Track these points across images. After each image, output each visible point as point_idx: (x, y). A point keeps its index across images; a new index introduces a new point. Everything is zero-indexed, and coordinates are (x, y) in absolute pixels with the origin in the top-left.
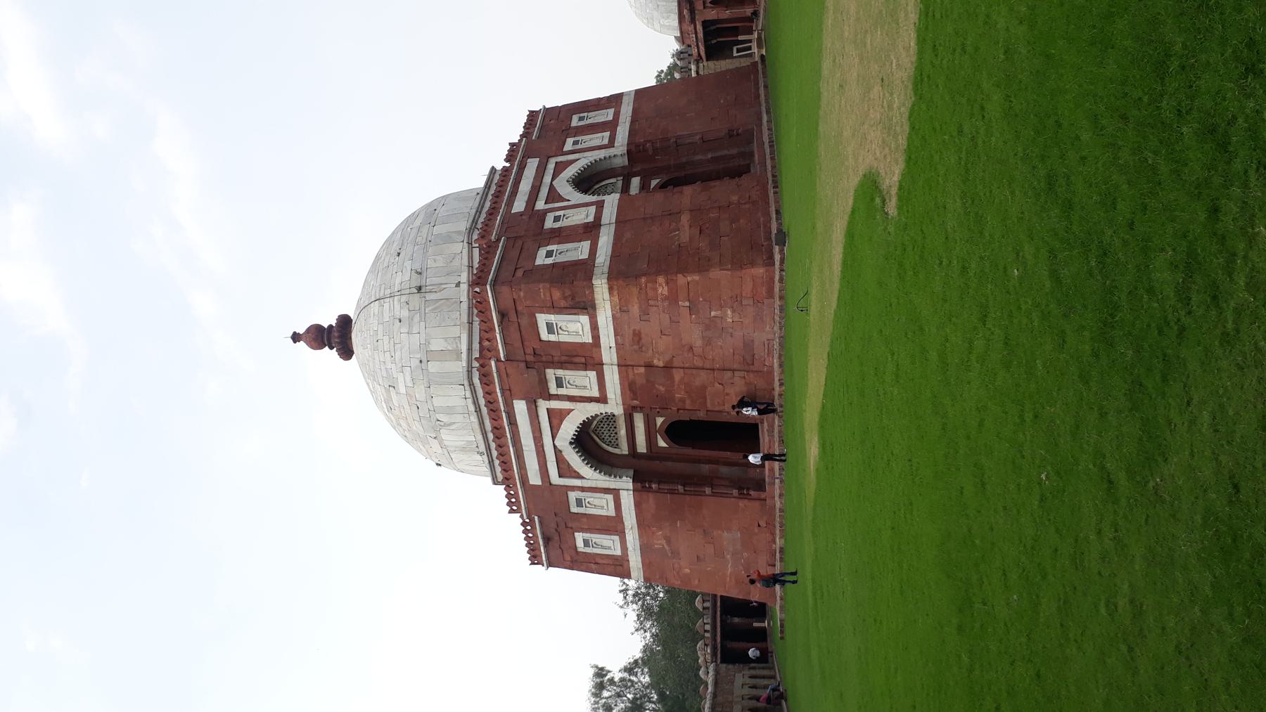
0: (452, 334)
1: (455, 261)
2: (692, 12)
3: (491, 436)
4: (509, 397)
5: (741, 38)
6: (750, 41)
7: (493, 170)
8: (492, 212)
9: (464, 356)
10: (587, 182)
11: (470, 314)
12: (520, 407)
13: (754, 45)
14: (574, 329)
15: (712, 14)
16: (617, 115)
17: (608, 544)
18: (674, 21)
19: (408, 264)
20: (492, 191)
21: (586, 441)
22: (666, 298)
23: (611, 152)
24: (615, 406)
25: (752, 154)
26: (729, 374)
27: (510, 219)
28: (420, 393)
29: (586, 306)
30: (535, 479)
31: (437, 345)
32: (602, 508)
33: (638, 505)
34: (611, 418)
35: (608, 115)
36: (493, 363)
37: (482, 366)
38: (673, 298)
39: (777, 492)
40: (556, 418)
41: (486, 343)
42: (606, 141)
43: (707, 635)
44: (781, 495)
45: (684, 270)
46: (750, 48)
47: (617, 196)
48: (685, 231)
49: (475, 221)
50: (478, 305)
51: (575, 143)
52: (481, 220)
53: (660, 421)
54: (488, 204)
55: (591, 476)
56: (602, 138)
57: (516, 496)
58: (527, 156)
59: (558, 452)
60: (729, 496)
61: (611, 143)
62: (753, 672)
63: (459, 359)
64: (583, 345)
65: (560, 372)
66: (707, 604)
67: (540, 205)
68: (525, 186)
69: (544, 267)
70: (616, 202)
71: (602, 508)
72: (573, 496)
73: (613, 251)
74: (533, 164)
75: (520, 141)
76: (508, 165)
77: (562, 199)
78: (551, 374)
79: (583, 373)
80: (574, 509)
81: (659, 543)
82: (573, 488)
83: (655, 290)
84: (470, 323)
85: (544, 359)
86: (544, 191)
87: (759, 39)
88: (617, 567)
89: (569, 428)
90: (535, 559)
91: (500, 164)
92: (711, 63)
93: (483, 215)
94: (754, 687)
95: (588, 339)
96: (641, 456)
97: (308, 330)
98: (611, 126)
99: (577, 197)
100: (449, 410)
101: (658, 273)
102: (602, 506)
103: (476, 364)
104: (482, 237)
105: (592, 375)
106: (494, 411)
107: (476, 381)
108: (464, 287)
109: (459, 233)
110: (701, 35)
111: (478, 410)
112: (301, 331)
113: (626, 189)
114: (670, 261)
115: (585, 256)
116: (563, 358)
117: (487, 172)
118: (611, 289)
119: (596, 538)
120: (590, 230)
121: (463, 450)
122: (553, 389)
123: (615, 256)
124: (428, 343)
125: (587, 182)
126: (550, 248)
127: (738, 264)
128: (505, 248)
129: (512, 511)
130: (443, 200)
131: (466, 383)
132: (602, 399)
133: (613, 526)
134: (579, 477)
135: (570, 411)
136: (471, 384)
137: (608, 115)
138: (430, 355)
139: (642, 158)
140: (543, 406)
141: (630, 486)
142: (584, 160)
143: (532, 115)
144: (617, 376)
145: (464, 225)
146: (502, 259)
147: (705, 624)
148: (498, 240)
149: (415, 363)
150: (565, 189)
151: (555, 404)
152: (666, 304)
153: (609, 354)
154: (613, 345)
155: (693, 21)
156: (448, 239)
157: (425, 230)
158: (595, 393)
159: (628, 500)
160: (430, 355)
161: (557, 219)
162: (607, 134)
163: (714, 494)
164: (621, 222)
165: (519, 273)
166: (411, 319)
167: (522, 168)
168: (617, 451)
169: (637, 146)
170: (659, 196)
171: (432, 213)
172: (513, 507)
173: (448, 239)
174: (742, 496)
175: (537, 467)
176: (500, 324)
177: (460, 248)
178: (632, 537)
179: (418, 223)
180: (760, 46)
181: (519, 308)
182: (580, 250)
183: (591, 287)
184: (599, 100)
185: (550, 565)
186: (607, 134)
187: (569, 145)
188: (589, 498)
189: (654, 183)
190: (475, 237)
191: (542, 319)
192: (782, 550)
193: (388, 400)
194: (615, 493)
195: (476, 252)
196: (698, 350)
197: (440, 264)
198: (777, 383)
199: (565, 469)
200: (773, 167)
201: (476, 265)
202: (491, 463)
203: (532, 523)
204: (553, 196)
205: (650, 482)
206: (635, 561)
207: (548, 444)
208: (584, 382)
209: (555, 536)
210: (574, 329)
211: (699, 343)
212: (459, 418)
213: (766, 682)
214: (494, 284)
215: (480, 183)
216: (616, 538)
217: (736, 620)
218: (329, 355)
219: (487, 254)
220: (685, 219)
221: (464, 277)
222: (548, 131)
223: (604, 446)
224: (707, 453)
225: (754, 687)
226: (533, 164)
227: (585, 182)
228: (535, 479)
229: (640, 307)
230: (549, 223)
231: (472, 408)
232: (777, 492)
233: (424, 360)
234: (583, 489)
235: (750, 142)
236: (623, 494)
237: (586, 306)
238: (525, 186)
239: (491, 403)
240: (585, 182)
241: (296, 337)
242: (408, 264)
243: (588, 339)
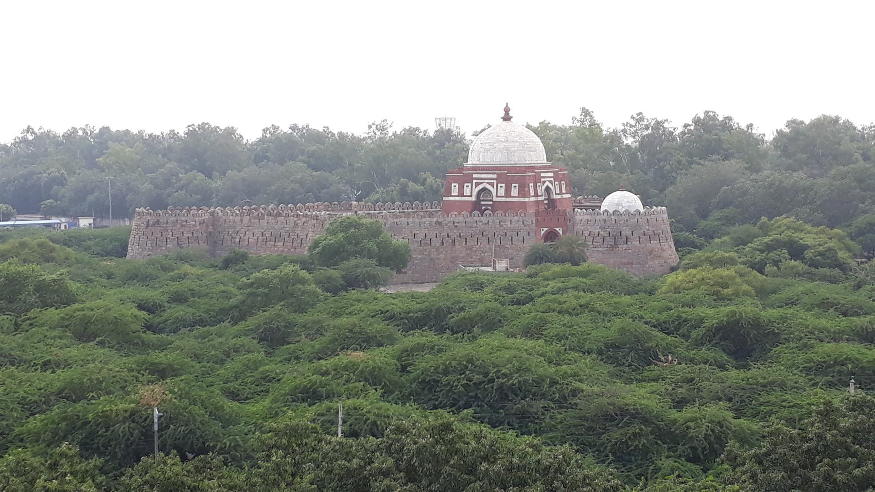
4: (498, 174)
10: (548, 189)
12: (495, 176)
14: (515, 192)
55: (476, 191)
56: (558, 192)
72: (469, 185)
89: (489, 187)
98: (561, 193)
99: (544, 188)
102: (467, 191)
120: (536, 195)
122: (499, 185)
125: (548, 189)
133: (461, 194)
140: (495, 182)
150: (545, 185)
178: (457, 199)
194: (471, 196)
199: (477, 184)
204: (544, 182)
208: (502, 192)
228: (475, 176)
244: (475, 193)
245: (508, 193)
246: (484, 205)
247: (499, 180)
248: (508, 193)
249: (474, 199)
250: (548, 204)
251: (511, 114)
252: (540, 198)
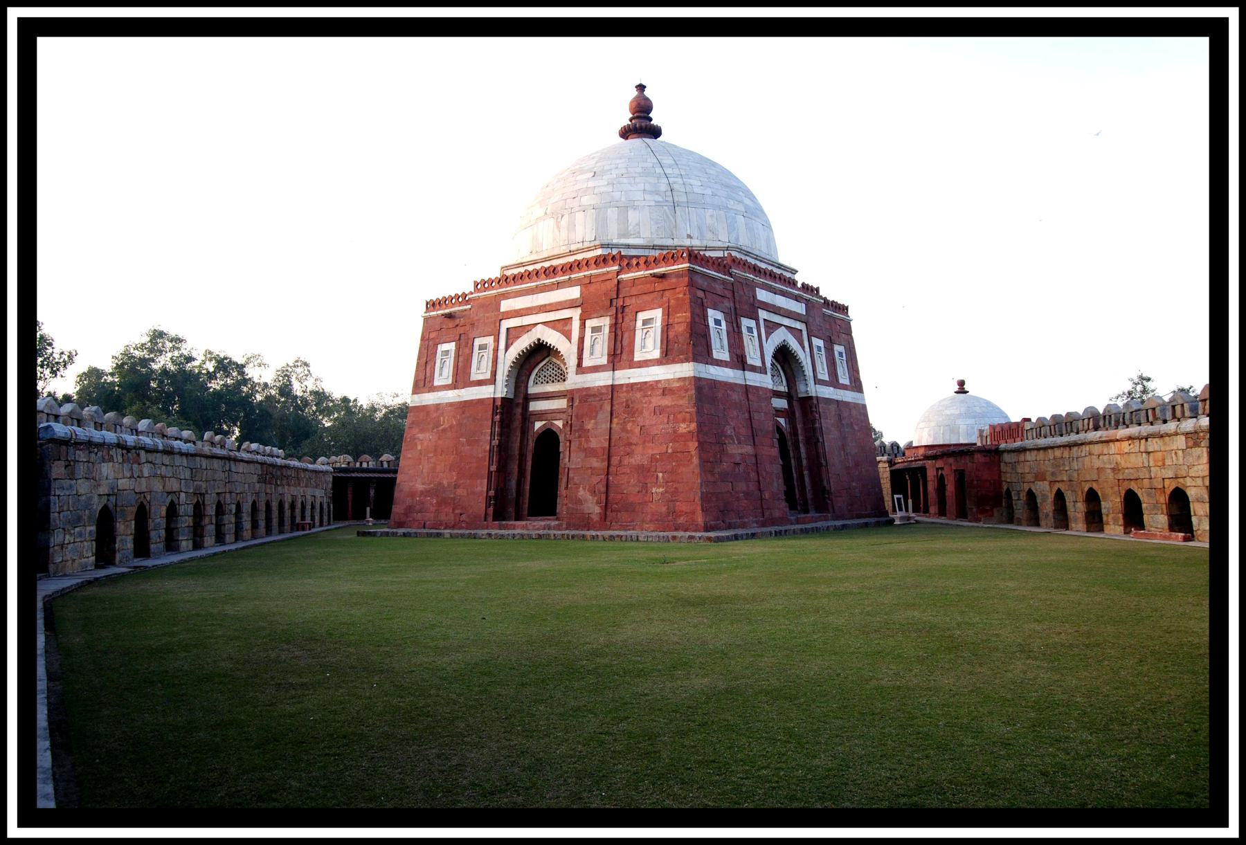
0: (642, 230)
1: (711, 233)
2: (935, 457)
3: (547, 265)
4: (586, 283)
5: (910, 501)
6: (907, 510)
7: (794, 272)
8: (756, 270)
9: (623, 241)
11: (661, 247)
12: (574, 293)
13: (903, 514)
14: (648, 343)
15: (931, 474)
16: (844, 387)
17: (443, 375)
18: (926, 440)
19: (708, 192)
20: (775, 270)
21: (540, 351)
22: (675, 432)
23: (811, 382)
24: (574, 381)
25: (807, 511)
26: (604, 489)
27: (752, 286)
28: (586, 200)
29: (668, 355)
30: (506, 305)
31: (633, 216)
32: (478, 369)
33: (481, 402)
34: (562, 377)
35: (844, 379)
36: (616, 268)
37: (613, 258)
38: (676, 437)
39: (493, 532)
40: (562, 326)
41: (634, 262)
42: (820, 377)
43: (358, 465)
44: (490, 535)
45: (702, 447)
46: (901, 510)
47: (770, 387)
48: (739, 450)
49: (748, 253)
50: (671, 255)
51: (819, 348)
52: (749, 260)
53: (559, 424)
54: (763, 266)
56: (824, 375)
57: (491, 287)
58: (807, 302)
60: (488, 489)
61: (817, 381)
62: (325, 506)
63: (620, 236)
64: (632, 352)
65: (607, 330)
66: (385, 465)
67: (763, 314)
68: (780, 301)
69: (705, 317)
70: (764, 385)
71: (478, 369)
73: (720, 382)
74: (800, 308)
75: (821, 297)
76: (799, 285)
77: (768, 335)
78: (605, 322)
79: (606, 352)
81: (446, 422)
82: (497, 341)
83: (684, 421)
84: (654, 247)
85: (620, 315)
86: (776, 319)
87: (909, 518)
88: (423, 382)
89: (553, 338)
90: (431, 305)
91: (800, 279)
92: (888, 475)
93: (753, 262)
94: (313, 507)
95: (638, 357)
96: (526, 407)
97: (647, 99)
98: (834, 382)
99: (769, 350)
100: (572, 226)
101: (700, 426)
102: (480, 370)
103: (615, 252)
104: (734, 260)
105: (604, 361)
106: (570, 268)
107: (599, 252)
108: (687, 243)
109: (737, 239)
110: (914, 465)
111: (571, 253)
112: (647, 93)
113: (778, 394)
114: (710, 437)
115: (716, 355)
116: (619, 333)
117: (793, 266)
118: (684, 379)
119: (450, 362)
120: (739, 361)
121: (535, 239)
122: (589, 323)
123: (714, 384)
124: (635, 208)
126: (723, 323)
127: (705, 498)
128: (724, 282)
129: (476, 284)
130: (767, 226)
131: (597, 243)
132: (580, 368)
134: (507, 348)
135: (569, 338)
136: (596, 248)
137: (844, 379)
138: (624, 209)
139: (804, 409)
141: (499, 395)
142: (803, 356)
143: (843, 309)
144: (602, 383)
145: (744, 242)
146: (714, 279)
147: (368, 462)
148: (731, 275)
149: (617, 195)
150: (779, 336)
151: (576, 325)
152: (670, 431)
153: (625, 376)
154: (632, 381)
155: (926, 458)
156: (732, 227)
157: (741, 208)
159: (486, 392)
160: (624, 209)
161: (750, 330)
162: (826, 378)
163: (490, 473)
164: (747, 389)
165: (700, 294)
166: (657, 193)
167: (797, 298)
168: (531, 382)
169: (817, 406)
170: (769, 426)
171: (755, 213)
172: (481, 285)
173: (732, 227)
174: (488, 498)
175: (517, 308)
176: (654, 276)
177: (723, 239)
178: (452, 396)
179: (747, 201)
180: (902, 518)
181: (667, 294)
182: (721, 351)
183: (687, 360)
184: (857, 371)
185: (426, 320)
186: (826, 378)
187: (818, 342)
188: (488, 355)
189: (782, 421)
190: (734, 254)
191: (657, 314)
192: (439, 535)
193: (582, 171)
194: (493, 381)
195: (720, 254)
196: (626, 461)
197: (709, 221)
198: (594, 533)
199: (513, 335)
200: (794, 532)
201: (708, 254)
202: (521, 265)
203: (468, 302)
204: (771, 327)
205: (502, 413)
206: (429, 399)
207: (537, 317)
208: (598, 353)
209: (452, 323)
210: (648, 343)
211: (632, 461)
212: (564, 234)
213: (317, 518)
214: (691, 271)
215: (782, 261)
216: (450, 381)
217: (372, 492)
218: (624, 118)
219: (718, 264)
220: (749, 449)
221: (696, 243)
222: (829, 322)
223: (536, 371)
224: (529, 468)
225: (313, 507)
226: (800, 308)
227: (784, 356)
228: (506, 305)
229: (667, 407)
230: (746, 323)
231: (573, 248)
232: (493, 532)
233: (620, 204)
234: (496, 350)
235: (818, 510)
236: (490, 388)
237: (668, 355)
238: (780, 301)
239: (578, 265)
240: (784, 356)
241: (641, 88)
242: (708, 192)
245: (619, 354)
246: (541, 415)
247: (588, 308)
248: (619, 354)
250: (789, 414)
251: (657, 118)
252: (754, 379)
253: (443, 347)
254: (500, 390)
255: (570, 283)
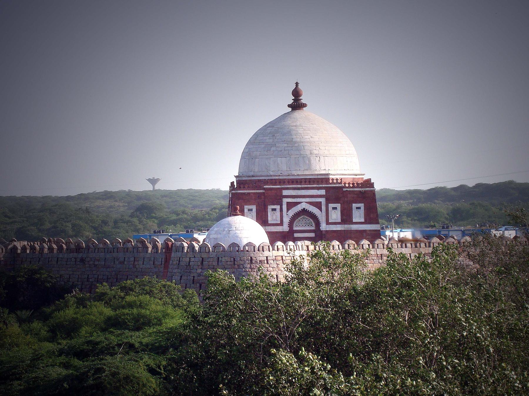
14: (358, 215)
40: (318, 205)
59: (299, 203)
72: (278, 207)
80: (270, 207)
95: (354, 220)
122: (331, 206)
158: (330, 221)
191: (362, 205)
194: (281, 224)
199: (290, 206)
208: (336, 216)
210: (358, 215)
241: (297, 84)
243: (354, 220)
244: (286, 220)
245: (346, 218)
249: (285, 228)
251: (304, 99)
253: (250, 207)
254: (285, 228)
255: (318, 189)
